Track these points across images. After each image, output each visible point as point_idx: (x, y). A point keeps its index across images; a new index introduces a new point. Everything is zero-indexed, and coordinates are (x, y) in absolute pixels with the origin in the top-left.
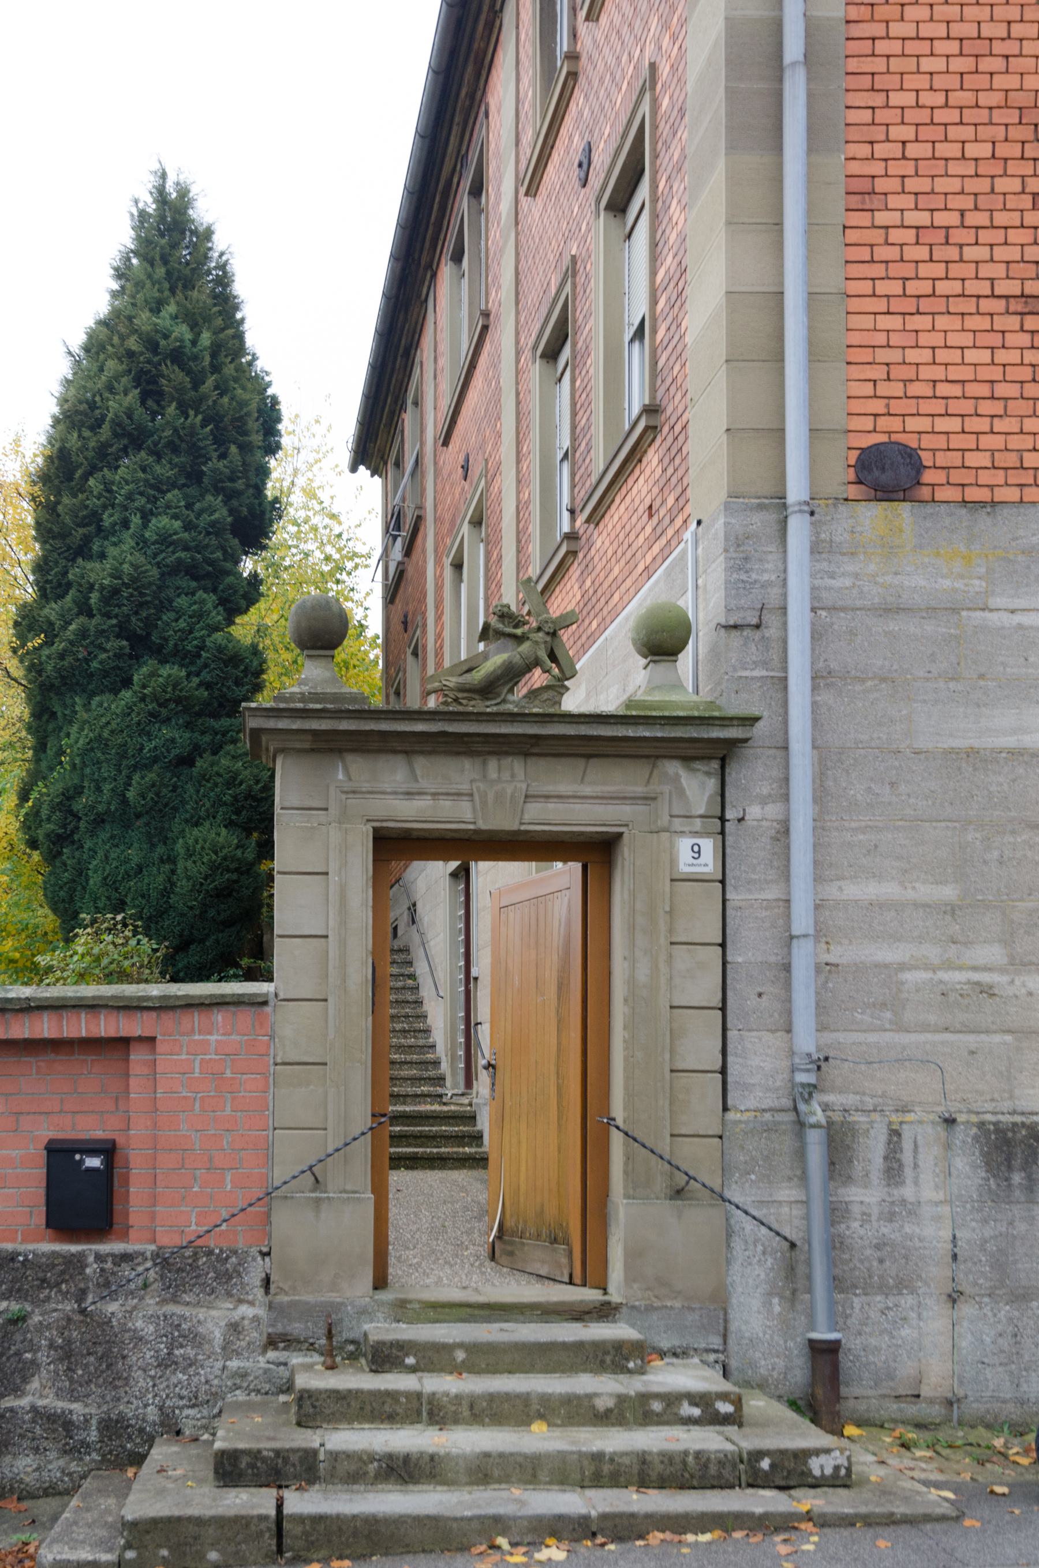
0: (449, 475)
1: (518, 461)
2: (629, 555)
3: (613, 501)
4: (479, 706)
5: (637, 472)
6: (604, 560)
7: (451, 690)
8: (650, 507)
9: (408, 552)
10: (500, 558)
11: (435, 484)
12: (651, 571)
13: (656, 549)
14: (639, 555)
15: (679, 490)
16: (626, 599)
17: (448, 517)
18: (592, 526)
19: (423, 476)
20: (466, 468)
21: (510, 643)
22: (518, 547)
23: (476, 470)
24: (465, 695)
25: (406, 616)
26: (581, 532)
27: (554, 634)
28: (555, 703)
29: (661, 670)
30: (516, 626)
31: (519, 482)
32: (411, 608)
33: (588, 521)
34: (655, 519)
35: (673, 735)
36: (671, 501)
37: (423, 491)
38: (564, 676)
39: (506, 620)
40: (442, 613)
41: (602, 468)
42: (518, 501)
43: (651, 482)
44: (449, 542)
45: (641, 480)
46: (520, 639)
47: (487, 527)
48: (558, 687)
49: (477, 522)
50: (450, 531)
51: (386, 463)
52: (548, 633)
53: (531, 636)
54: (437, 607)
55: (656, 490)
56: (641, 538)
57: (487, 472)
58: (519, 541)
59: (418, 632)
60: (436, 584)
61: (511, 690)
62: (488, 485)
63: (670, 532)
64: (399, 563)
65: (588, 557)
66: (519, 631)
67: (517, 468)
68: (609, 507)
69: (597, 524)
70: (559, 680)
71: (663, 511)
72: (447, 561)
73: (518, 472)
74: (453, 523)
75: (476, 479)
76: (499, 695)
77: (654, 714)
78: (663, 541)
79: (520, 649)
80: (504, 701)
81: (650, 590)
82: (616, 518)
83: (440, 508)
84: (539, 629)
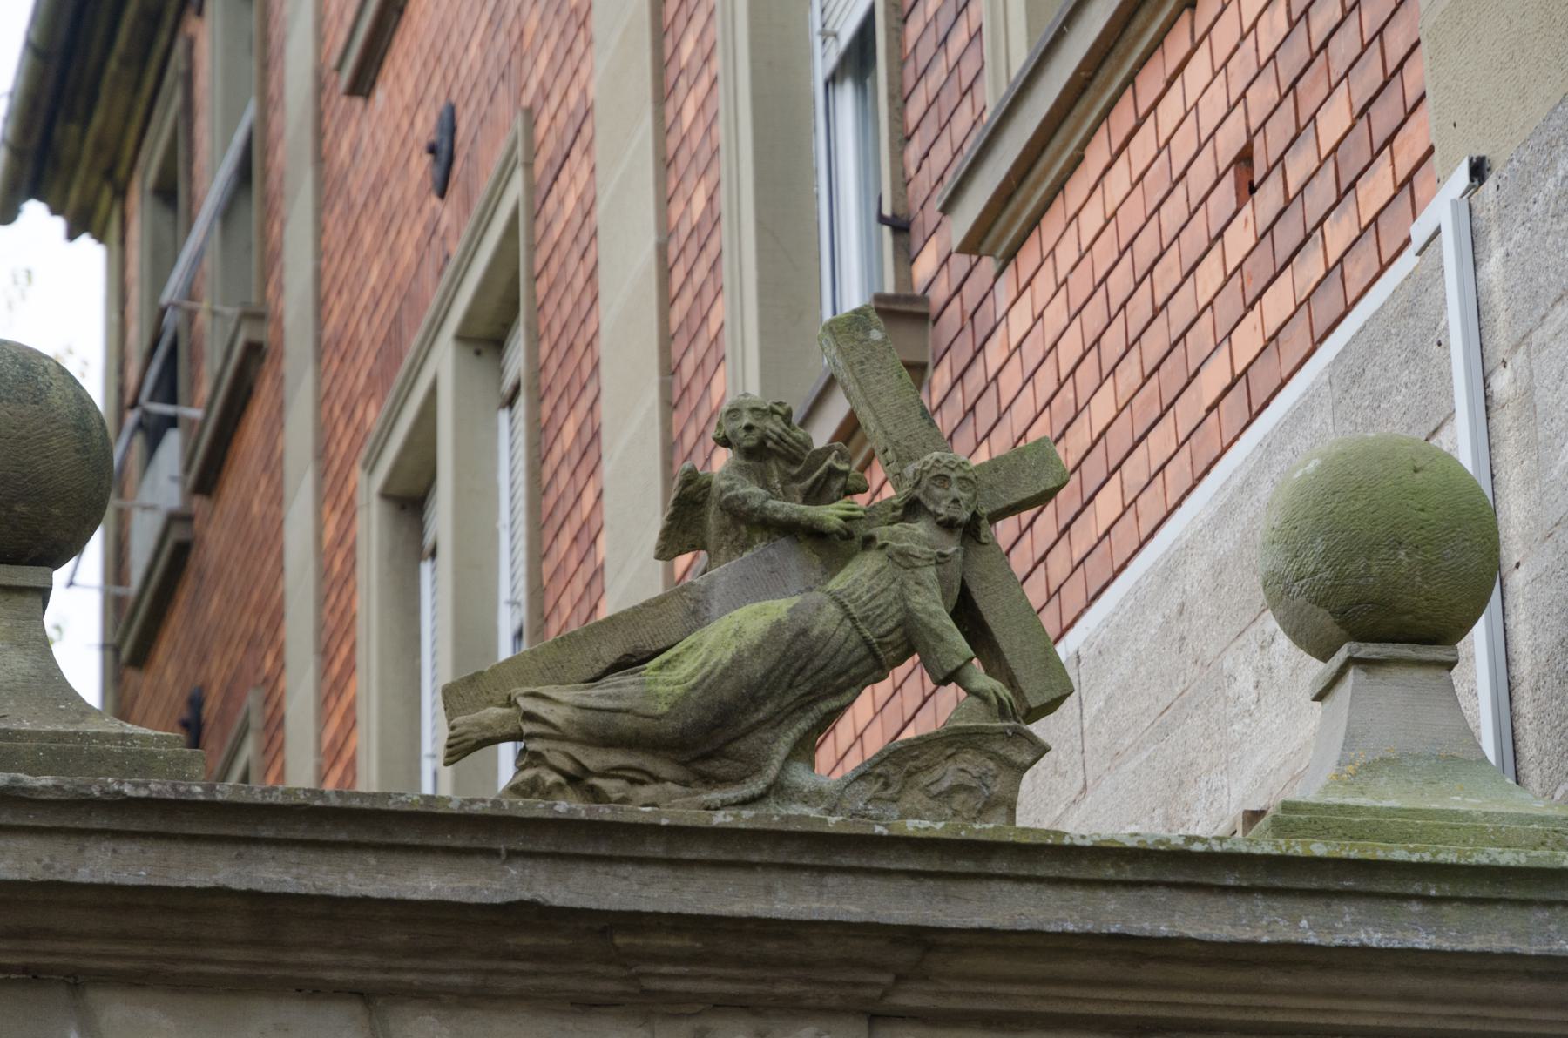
0: (376, 191)
1: (662, 94)
2: (1155, 342)
3: (1077, 161)
4: (668, 802)
5: (1178, 44)
6: (1046, 381)
7: (558, 735)
8: (1244, 158)
9: (208, 476)
10: (592, 440)
11: (320, 230)
12: (1262, 382)
13: (1278, 303)
14: (1201, 338)
15: (1370, 75)
16: (1151, 507)
17: (369, 333)
18: (988, 265)
19: (270, 212)
20: (443, 153)
21: (792, 559)
22: (665, 388)
23: (482, 155)
24: (616, 758)
25: (196, 702)
26: (939, 294)
27: (971, 531)
28: (990, 805)
29: (1388, 700)
30: (816, 494)
31: (664, 163)
32: (217, 672)
33: (973, 244)
34: (1269, 198)
35: (1475, 944)
36: (1334, 120)
37: (270, 260)
38: (1018, 705)
39: (775, 470)
40: (350, 667)
41: (1021, 58)
42: (666, 232)
43: (1242, 69)
44: (373, 416)
45: (1199, 69)
46: (834, 547)
47: (535, 339)
48: (1008, 731)
49: (486, 339)
50: (378, 380)
51: (121, 193)
52: (948, 525)
53: (882, 532)
54: (325, 653)
55: (1263, 95)
56: (1210, 275)
57: (532, 153)
58: (669, 369)
59: (249, 750)
60: (323, 572)
61: (805, 749)
62: (537, 197)
63: (1339, 233)
64: (173, 519)
65: (975, 379)
66: (830, 514)
67: (659, 116)
68: (1059, 187)
69: (1011, 256)
70: (1003, 711)
71: (1300, 165)
72: (368, 487)
73: (662, 130)
74: (391, 348)
75: (484, 186)
76: (754, 766)
77: (1399, 854)
78: (1310, 268)
79: (837, 583)
80: (777, 789)
81: (1269, 447)
82: (1091, 220)
83: (337, 307)
84: (912, 508)
